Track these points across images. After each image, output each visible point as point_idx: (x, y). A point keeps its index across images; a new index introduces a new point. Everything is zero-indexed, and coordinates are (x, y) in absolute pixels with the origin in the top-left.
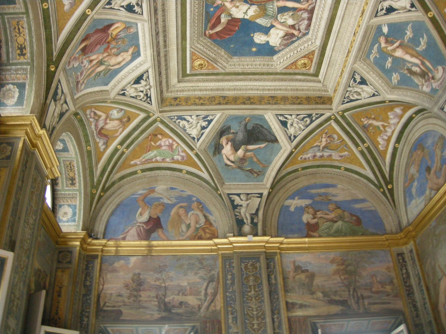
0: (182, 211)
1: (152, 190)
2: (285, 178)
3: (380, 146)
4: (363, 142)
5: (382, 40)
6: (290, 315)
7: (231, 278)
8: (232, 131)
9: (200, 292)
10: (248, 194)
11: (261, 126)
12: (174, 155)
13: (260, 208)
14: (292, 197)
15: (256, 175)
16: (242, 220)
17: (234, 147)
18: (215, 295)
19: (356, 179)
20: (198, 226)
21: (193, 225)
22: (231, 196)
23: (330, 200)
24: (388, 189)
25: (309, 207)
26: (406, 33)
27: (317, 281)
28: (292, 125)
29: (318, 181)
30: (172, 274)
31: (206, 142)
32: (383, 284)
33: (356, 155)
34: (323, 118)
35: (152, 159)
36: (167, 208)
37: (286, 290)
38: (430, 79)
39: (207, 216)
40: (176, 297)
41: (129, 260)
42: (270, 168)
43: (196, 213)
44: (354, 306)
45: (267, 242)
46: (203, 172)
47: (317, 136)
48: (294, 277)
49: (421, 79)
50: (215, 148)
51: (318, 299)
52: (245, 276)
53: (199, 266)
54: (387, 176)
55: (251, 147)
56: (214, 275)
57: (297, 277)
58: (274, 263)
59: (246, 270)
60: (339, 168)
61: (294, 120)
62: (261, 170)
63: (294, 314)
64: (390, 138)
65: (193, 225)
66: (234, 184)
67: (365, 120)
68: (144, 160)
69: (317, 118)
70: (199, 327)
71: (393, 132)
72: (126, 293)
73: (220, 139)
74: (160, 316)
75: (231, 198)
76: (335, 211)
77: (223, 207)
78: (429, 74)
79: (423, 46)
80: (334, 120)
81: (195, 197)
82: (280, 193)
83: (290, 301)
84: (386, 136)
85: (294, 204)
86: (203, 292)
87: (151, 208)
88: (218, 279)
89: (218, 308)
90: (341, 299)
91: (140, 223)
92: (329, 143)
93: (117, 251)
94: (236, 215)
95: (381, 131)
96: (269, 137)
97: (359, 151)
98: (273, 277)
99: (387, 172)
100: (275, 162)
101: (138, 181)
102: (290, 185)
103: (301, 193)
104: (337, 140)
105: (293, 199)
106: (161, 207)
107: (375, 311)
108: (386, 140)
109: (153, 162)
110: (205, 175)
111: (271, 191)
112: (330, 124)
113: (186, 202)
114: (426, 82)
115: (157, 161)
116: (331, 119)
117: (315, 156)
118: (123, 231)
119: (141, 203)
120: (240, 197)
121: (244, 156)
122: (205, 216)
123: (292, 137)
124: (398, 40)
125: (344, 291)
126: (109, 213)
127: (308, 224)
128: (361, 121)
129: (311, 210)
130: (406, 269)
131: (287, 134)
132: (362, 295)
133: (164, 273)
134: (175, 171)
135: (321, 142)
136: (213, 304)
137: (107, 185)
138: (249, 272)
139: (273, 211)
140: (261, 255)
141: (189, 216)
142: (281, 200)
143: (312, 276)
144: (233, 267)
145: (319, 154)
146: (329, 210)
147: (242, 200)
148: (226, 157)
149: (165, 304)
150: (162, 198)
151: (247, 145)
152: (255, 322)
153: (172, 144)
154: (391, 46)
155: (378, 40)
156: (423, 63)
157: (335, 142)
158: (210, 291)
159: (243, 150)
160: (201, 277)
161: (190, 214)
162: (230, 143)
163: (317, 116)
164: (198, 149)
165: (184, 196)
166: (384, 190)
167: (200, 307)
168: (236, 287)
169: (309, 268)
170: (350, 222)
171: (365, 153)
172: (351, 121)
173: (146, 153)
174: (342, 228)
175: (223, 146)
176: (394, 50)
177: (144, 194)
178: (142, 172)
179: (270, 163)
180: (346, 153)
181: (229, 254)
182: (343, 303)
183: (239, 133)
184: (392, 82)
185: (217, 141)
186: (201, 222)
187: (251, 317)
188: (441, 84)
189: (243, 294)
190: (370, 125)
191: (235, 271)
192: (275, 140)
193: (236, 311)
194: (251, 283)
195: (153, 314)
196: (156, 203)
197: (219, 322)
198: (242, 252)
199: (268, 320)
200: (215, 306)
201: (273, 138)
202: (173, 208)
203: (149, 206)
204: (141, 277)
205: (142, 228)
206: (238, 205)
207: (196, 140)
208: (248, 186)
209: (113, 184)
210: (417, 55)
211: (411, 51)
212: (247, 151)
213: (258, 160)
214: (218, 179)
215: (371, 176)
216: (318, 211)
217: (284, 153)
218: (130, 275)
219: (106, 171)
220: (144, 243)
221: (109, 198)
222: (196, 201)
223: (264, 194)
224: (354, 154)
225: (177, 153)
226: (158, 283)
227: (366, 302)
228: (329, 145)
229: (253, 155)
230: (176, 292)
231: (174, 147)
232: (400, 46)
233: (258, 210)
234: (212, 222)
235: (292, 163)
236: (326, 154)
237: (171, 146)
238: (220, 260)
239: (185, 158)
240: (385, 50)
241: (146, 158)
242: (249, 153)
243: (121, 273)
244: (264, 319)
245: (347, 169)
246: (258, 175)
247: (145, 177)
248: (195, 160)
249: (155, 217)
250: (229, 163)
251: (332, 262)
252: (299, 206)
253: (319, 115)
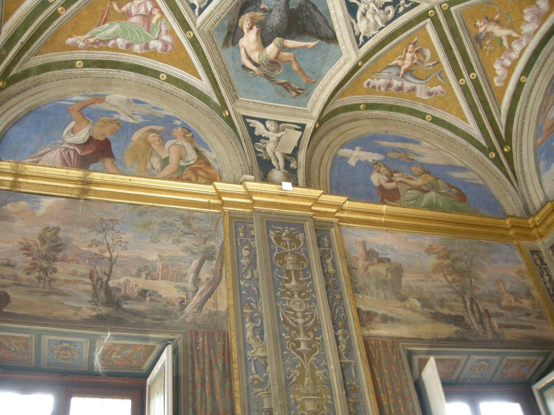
0: (152, 137)
1: (101, 99)
2: (338, 116)
3: (495, 80)
4: (470, 69)
6: (366, 333)
7: (249, 255)
8: (262, 6)
9: (185, 275)
10: (279, 123)
11: (313, 5)
12: (151, 39)
13: (300, 147)
14: (352, 145)
15: (294, 94)
16: (270, 161)
17: (262, 38)
18: (215, 283)
19: (449, 138)
20: (182, 164)
21: (173, 159)
22: (248, 120)
23: (413, 160)
24: (505, 154)
25: (380, 164)
27: (407, 279)
28: (364, 15)
29: (393, 130)
30: (127, 236)
31: (214, 19)
32: (516, 295)
33: (454, 93)
34: (415, 11)
35: (109, 41)
36: (126, 129)
37: (355, 290)
39: (201, 151)
40: (133, 281)
41: (39, 202)
42: (320, 86)
43: (180, 143)
44: (476, 327)
45: (316, 201)
46: (200, 78)
47: (399, 46)
48: (366, 269)
50: (229, 33)
51: (412, 309)
52: (276, 253)
53: (185, 229)
54: (502, 132)
55: (290, 43)
56: (214, 247)
57: (371, 269)
58: (329, 238)
59: (278, 243)
60: (422, 115)
61: (368, 6)
62: (303, 87)
63: (373, 332)
64: (515, 63)
65: (173, 159)
66: (255, 103)
67: (482, 24)
68: (92, 40)
69: (406, 10)
70: (180, 343)
71: (523, 51)
72: (22, 261)
73: (239, 18)
74: (95, 313)
75: (250, 123)
76: (422, 176)
77: (232, 141)
80: (431, 18)
81: (179, 120)
82: (332, 135)
83: (363, 308)
84: (510, 59)
85: (355, 156)
86: (191, 277)
87: (93, 124)
88: (222, 255)
89: (222, 308)
90: (453, 314)
91: (69, 144)
92: (416, 64)
93: (14, 184)
94: (257, 152)
95: (503, 49)
96: (324, 30)
97: (460, 85)
98: (329, 261)
99: (501, 126)
100: (329, 77)
101: (75, 81)
102: (346, 127)
103: (365, 142)
104: (429, 61)
105: (354, 149)
106: (114, 125)
107: (513, 338)
108: (507, 68)
109: (108, 49)
110: (203, 84)
111: (319, 127)
112: (424, 27)
113: (163, 126)
115: (115, 48)
116: (428, 17)
117: (389, 85)
118: (32, 153)
119: (75, 115)
120: (265, 125)
121: (276, 57)
122: (197, 151)
123: (361, 39)
125: (456, 301)
126: (9, 119)
127: (381, 187)
128: (476, 26)
129: (382, 169)
130: (548, 275)
131: (354, 32)
132: (486, 311)
133: (110, 233)
134: (146, 74)
135: (404, 59)
136: (211, 300)
137: (14, 72)
138: (286, 246)
139: (322, 159)
140: (305, 221)
141: (167, 146)
142: (334, 144)
143: (398, 271)
144: (253, 236)
145: (396, 83)
146: (412, 173)
147: (268, 130)
148: (246, 52)
149: (108, 291)
150: (116, 113)
151: (285, 38)
152: (302, 338)
153: (151, 13)
157: (426, 65)
158: (205, 275)
159: (277, 46)
160: (187, 249)
161: (168, 144)
162: (255, 29)
163: (406, 6)
164: (198, 29)
165: (158, 115)
166: (497, 155)
167: (183, 304)
168: (259, 271)
169: (391, 256)
170: (450, 196)
171: (469, 90)
172: (458, 25)
173: (99, 25)
174: (437, 202)
175: (243, 32)
177: (83, 101)
178: (84, 66)
179: (320, 77)
180: (439, 88)
181: (244, 213)
182: (457, 320)
183: (274, 13)
185: (234, 20)
186: (188, 159)
187: (292, 328)
189: (274, 284)
190: (489, 35)
191: (256, 244)
192: (332, 39)
193: (261, 316)
194: (290, 267)
195: (79, 309)
196: (106, 118)
197: (225, 336)
198: (271, 213)
199: (328, 336)
200: (215, 305)
201: (329, 33)
202: (136, 130)
203: (91, 121)
204: (61, 235)
205: (72, 153)
206: (260, 137)
207: (197, 10)
208: (280, 110)
209: (26, 74)
212: (283, 48)
213: (300, 69)
214: (228, 89)
215: (475, 132)
216: (396, 172)
217: (345, 63)
218: (38, 230)
219: (17, 42)
220: (76, 174)
221: (13, 96)
222: (180, 125)
223: (307, 127)
224: (452, 90)
225: (156, 36)
226: (95, 250)
227: (495, 322)
228: (415, 68)
229: (292, 59)
230: (134, 271)
231: (154, 21)
233: (296, 149)
234: (211, 161)
235: (353, 91)
236: (407, 85)
237: (147, 17)
238: (227, 222)
239: (170, 48)
241: (98, 37)
242: (286, 54)
243: (18, 224)
244: (319, 333)
245: (435, 120)
246: (298, 94)
247: (89, 75)
248: (187, 53)
249: (101, 139)
250: (249, 65)
251: (429, 250)
252: (363, 160)
253: (409, 5)
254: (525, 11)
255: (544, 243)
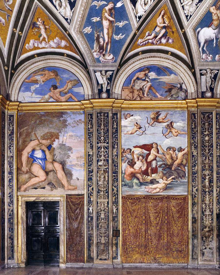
5: (111, 6)
26: (120, 22)
38: (102, 54)
49: (98, 48)
78: (104, 51)
79: (118, 38)
114: (98, 52)
124: (114, 18)
154: (108, 15)
155: (110, 2)
156: (107, 44)
176: (107, 19)
184: (83, 29)
188: (105, 62)
210: (110, 37)
211: (110, 32)
232: (111, 22)
240: (104, 12)
254: (57, 38)
255: (8, 112)
